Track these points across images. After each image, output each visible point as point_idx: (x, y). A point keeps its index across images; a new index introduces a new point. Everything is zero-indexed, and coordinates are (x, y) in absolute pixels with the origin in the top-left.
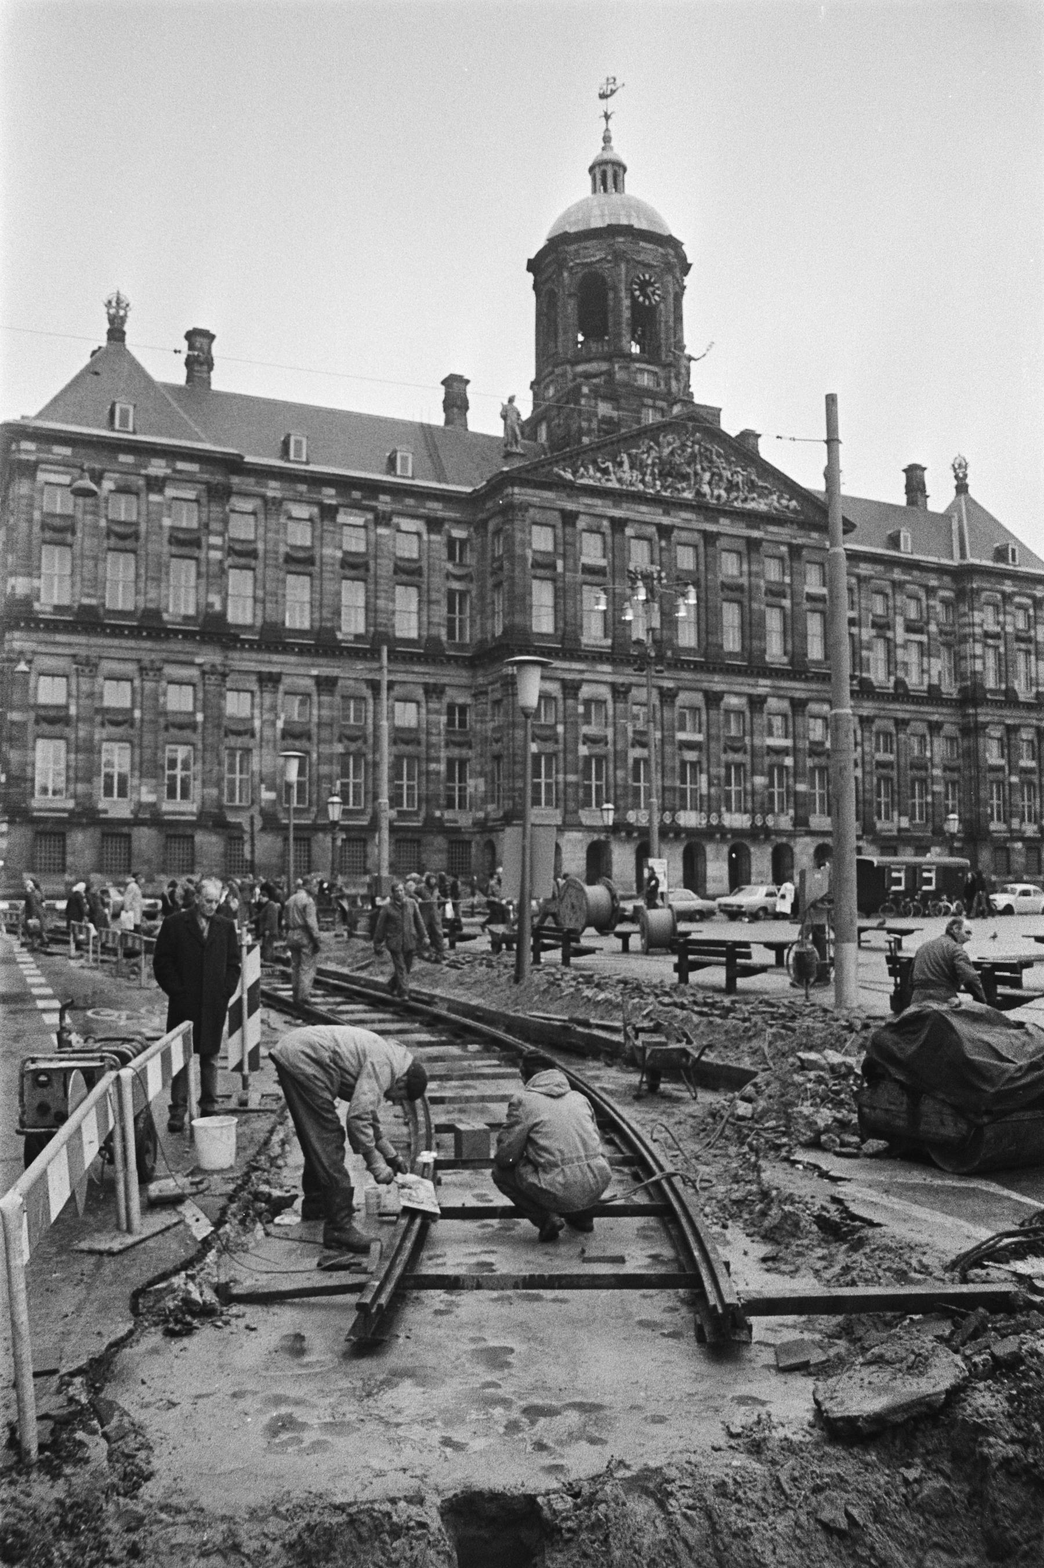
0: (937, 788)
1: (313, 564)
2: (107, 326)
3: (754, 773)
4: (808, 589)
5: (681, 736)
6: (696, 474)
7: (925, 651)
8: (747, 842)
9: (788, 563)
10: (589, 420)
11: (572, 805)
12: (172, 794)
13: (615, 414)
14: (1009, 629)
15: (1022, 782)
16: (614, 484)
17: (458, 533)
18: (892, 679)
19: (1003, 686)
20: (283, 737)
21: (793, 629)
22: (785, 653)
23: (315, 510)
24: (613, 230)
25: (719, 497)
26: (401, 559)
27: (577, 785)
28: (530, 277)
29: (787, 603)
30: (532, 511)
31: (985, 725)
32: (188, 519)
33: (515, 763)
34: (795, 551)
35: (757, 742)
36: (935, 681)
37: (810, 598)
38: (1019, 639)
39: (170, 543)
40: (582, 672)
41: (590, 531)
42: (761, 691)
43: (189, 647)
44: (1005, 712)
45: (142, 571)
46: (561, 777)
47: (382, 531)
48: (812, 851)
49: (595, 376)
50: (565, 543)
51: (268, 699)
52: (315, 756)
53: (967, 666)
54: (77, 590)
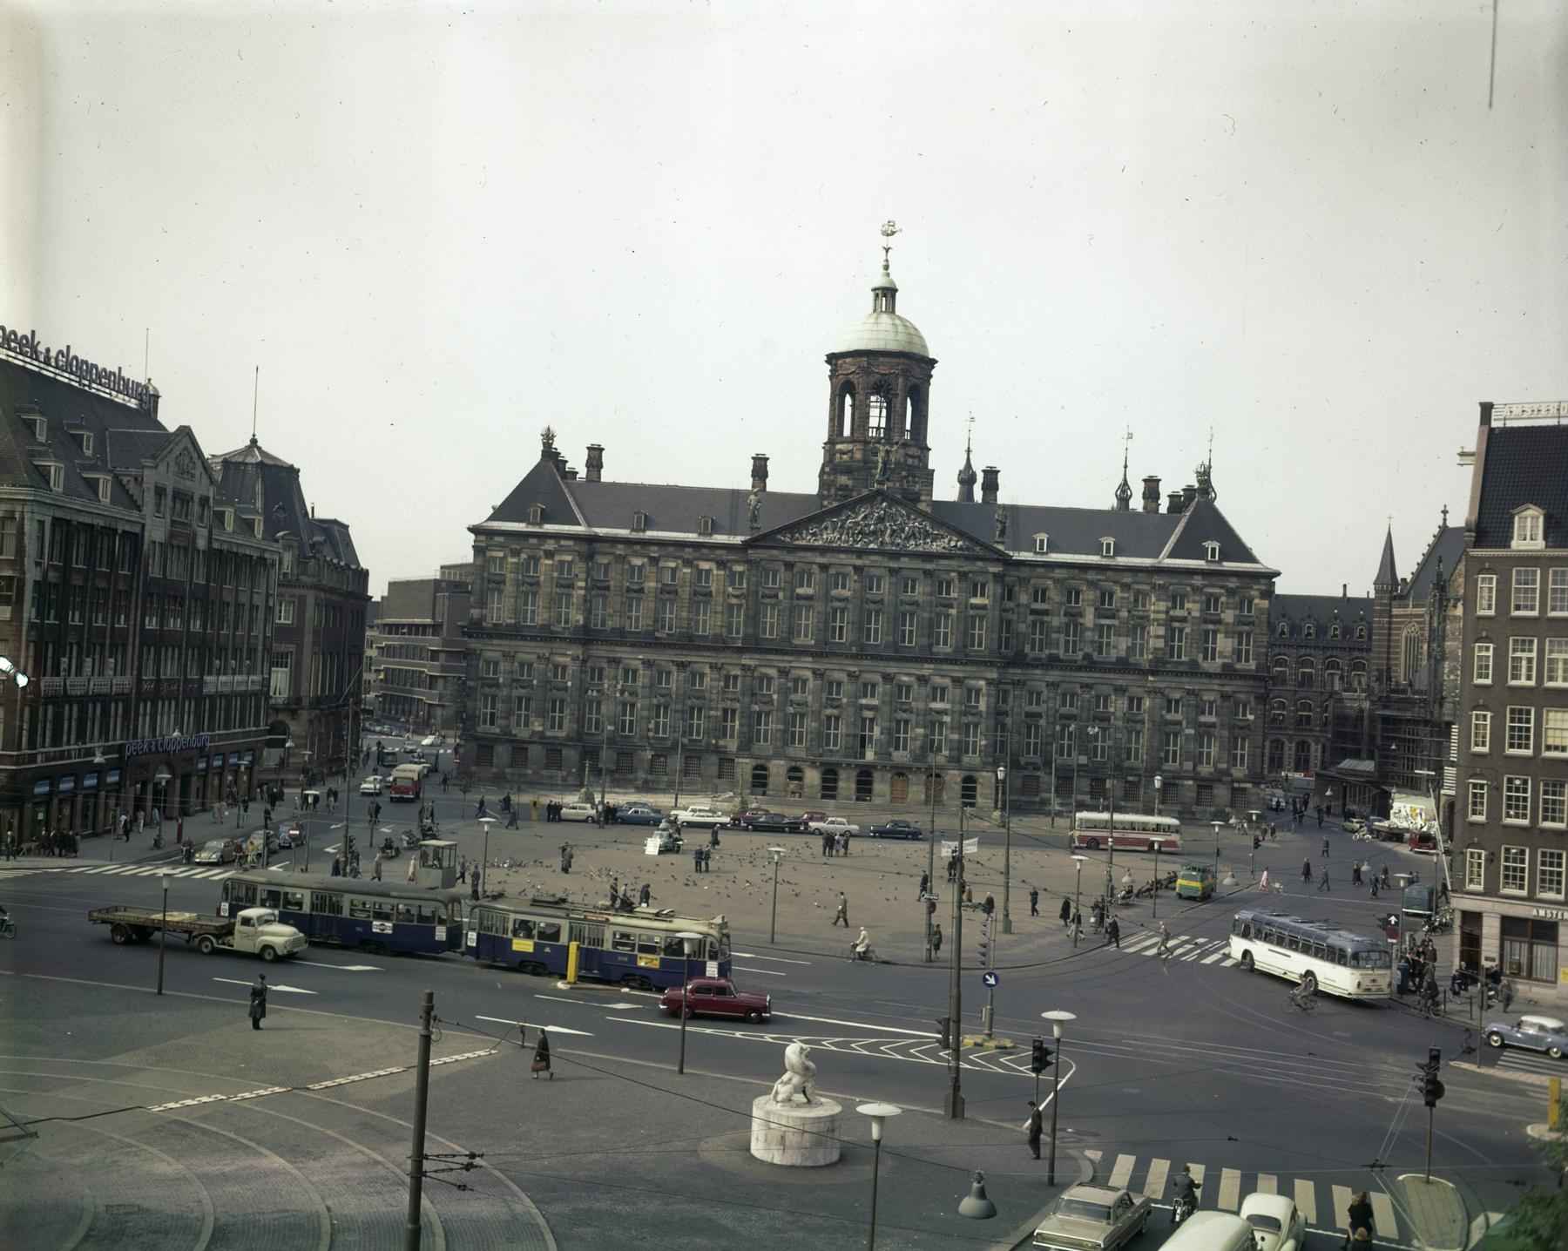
4: (973, 601)
5: (864, 701)
11: (779, 744)
12: (553, 727)
13: (850, 483)
14: (1196, 614)
18: (1080, 654)
27: (785, 731)
29: (953, 611)
34: (963, 576)
35: (921, 705)
36: (1123, 654)
38: (1206, 621)
42: (926, 672)
44: (1183, 679)
51: (613, 671)
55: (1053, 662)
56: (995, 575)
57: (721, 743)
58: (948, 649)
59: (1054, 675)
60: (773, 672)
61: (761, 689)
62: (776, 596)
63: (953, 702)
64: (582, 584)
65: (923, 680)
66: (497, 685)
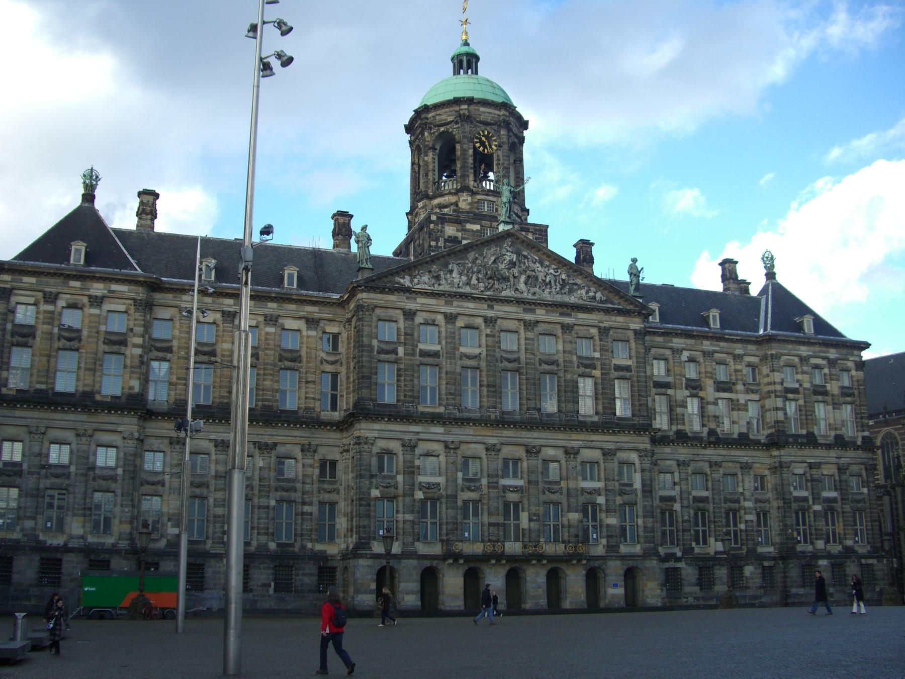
0: (749, 517)
1: (215, 356)
2: (83, 191)
3: (569, 511)
4: (614, 361)
6: (515, 277)
7: (735, 406)
8: (563, 566)
9: (598, 342)
10: (437, 240)
11: (410, 539)
13: (459, 235)
14: (807, 385)
15: (825, 511)
16: (444, 287)
17: (333, 329)
18: (706, 430)
19: (804, 432)
21: (604, 395)
22: (597, 413)
23: (218, 316)
24: (457, 101)
25: (534, 294)
26: (284, 350)
27: (413, 522)
28: (408, 137)
29: (597, 373)
30: (378, 311)
31: (788, 465)
32: (117, 325)
33: (360, 505)
34: (604, 332)
35: (572, 484)
36: (744, 430)
37: (618, 368)
39: (104, 343)
40: (418, 433)
41: (426, 323)
42: (575, 444)
43: (113, 418)
44: (807, 452)
45: (82, 365)
46: (400, 517)
47: (271, 330)
48: (622, 572)
50: (406, 334)
52: (211, 500)
53: (770, 417)
54: (35, 378)
55: (682, 438)
56: (635, 331)
57: (319, 547)
58: (596, 419)
59: (683, 452)
60: (395, 446)
61: (381, 469)
62: (395, 352)
63: (606, 480)
64: (138, 340)
65: (571, 453)
66: (20, 474)
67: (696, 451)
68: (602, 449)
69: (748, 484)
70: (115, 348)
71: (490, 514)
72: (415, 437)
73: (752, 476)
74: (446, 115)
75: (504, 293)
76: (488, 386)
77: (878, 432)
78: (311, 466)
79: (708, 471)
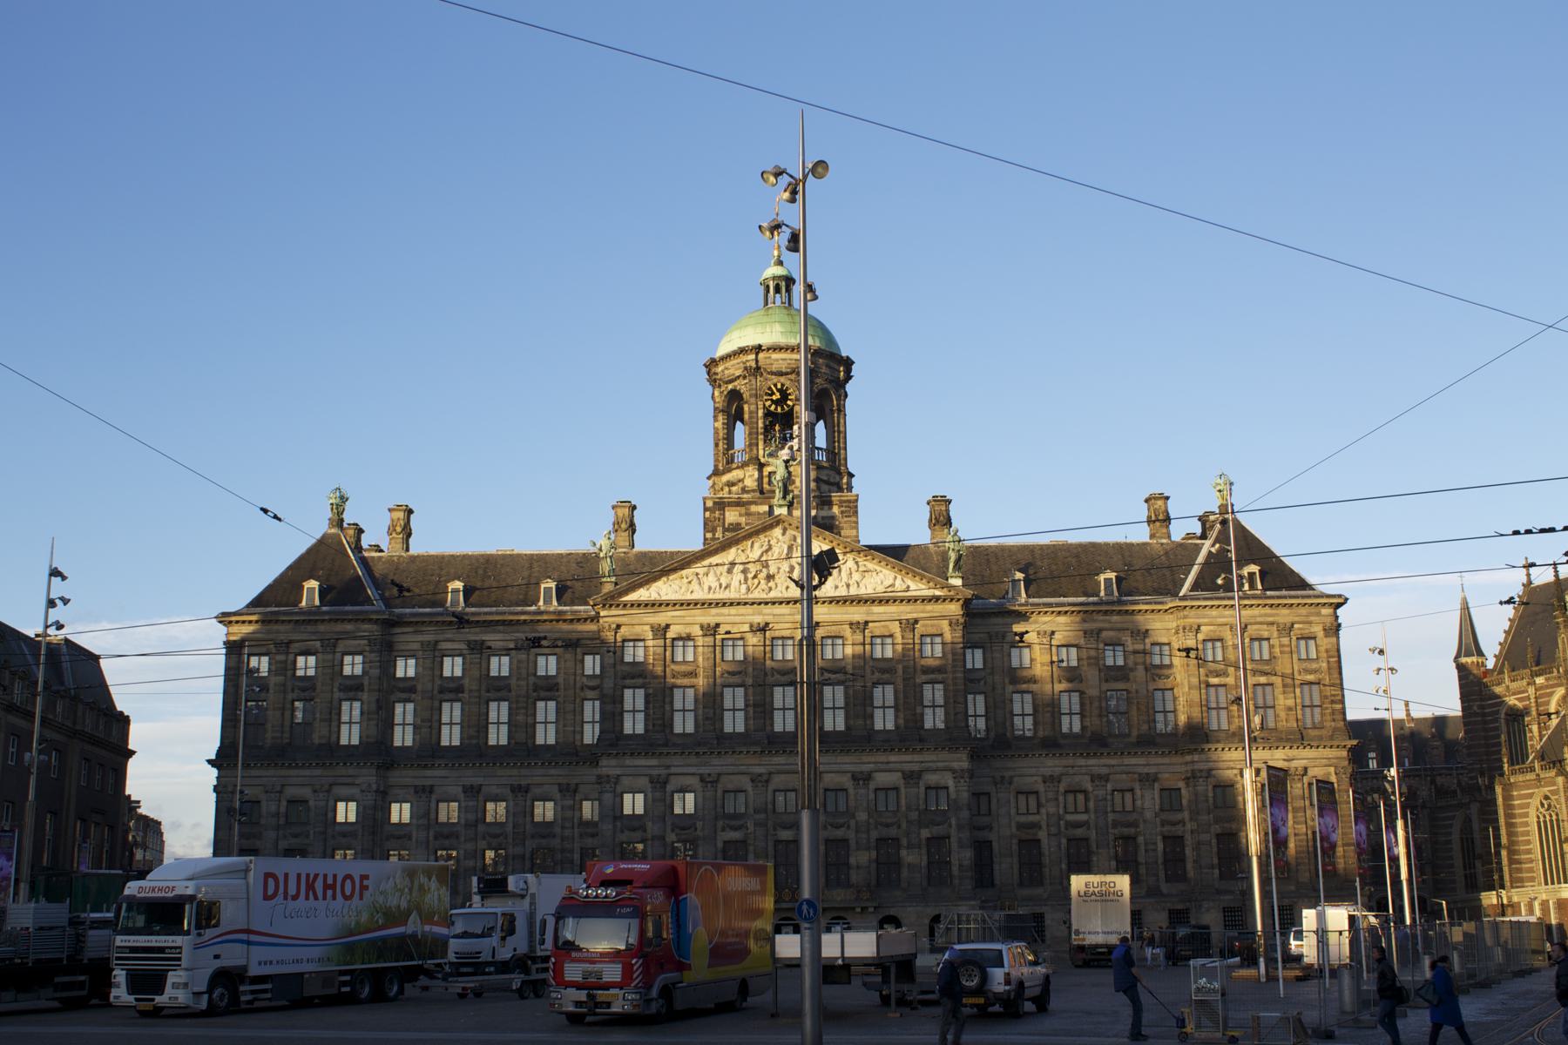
10: (714, 531)
13: (743, 520)
16: (699, 595)
20: (436, 838)
24: (742, 351)
42: (866, 768)
43: (351, 771)
48: (927, 921)
49: (733, 484)
59: (1051, 765)
65: (862, 779)
67: (1070, 761)
68: (903, 772)
69: (1149, 801)
70: (351, 694)
71: (757, 857)
72: (663, 772)
73: (1157, 792)
74: (733, 368)
75: (773, 594)
76: (755, 706)
77: (1551, 694)
78: (572, 808)
79: (1089, 787)
